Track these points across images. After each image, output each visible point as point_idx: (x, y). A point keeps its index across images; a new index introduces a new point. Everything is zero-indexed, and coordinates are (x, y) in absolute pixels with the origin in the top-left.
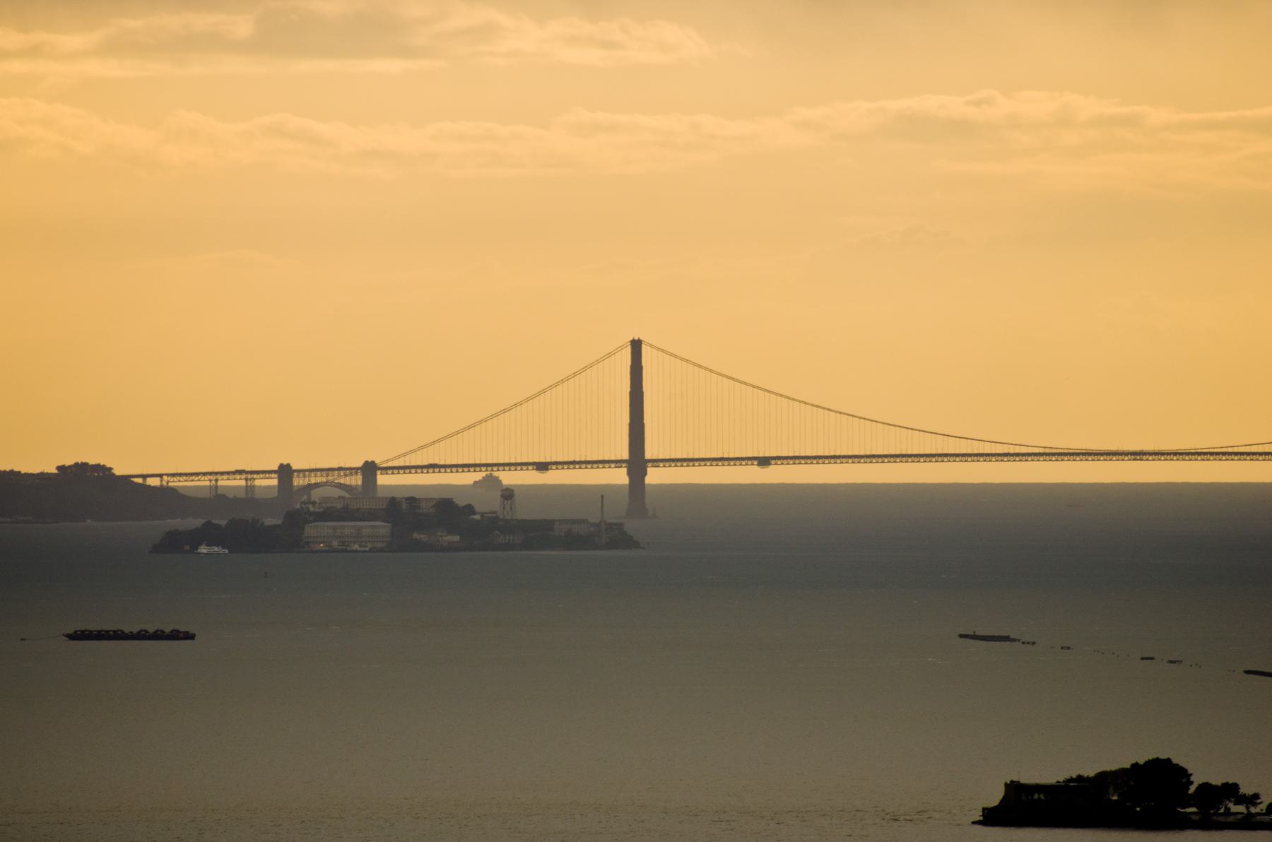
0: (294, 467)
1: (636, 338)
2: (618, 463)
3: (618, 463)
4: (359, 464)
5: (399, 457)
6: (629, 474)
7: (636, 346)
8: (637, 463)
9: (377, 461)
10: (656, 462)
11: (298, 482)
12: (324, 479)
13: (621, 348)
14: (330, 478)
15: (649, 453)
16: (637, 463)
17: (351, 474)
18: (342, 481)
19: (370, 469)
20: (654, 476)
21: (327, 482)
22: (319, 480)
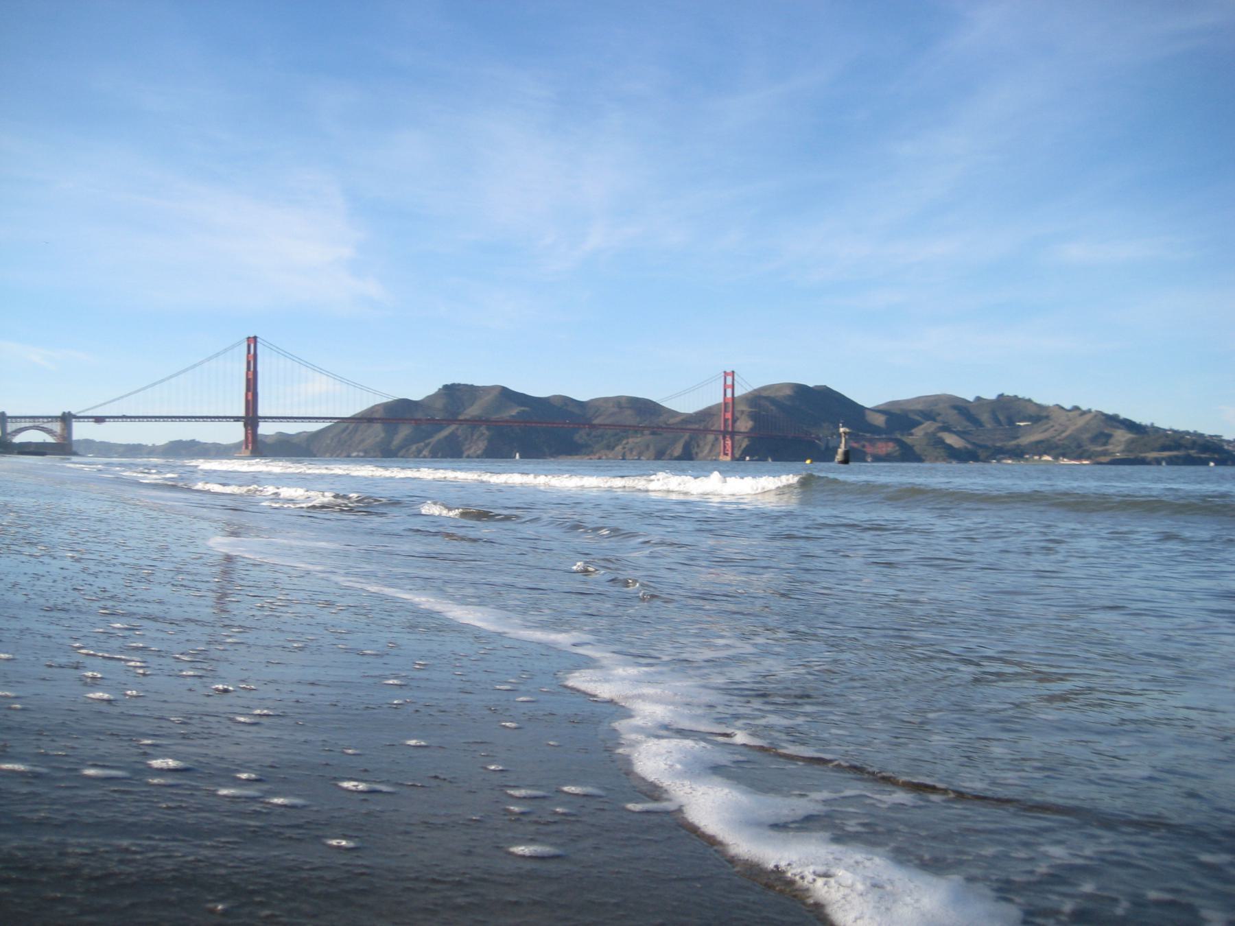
0: (9, 414)
1: (252, 336)
2: (237, 419)
3: (237, 419)
4: (59, 414)
5: (87, 410)
6: (246, 426)
7: (254, 340)
8: (251, 419)
9: (73, 412)
10: (265, 418)
11: (11, 427)
12: (31, 424)
13: (239, 344)
14: (37, 424)
15: (261, 413)
16: (251, 419)
17: (52, 422)
18: (45, 425)
19: (66, 419)
20: (265, 429)
21: (34, 426)
22: (27, 425)
